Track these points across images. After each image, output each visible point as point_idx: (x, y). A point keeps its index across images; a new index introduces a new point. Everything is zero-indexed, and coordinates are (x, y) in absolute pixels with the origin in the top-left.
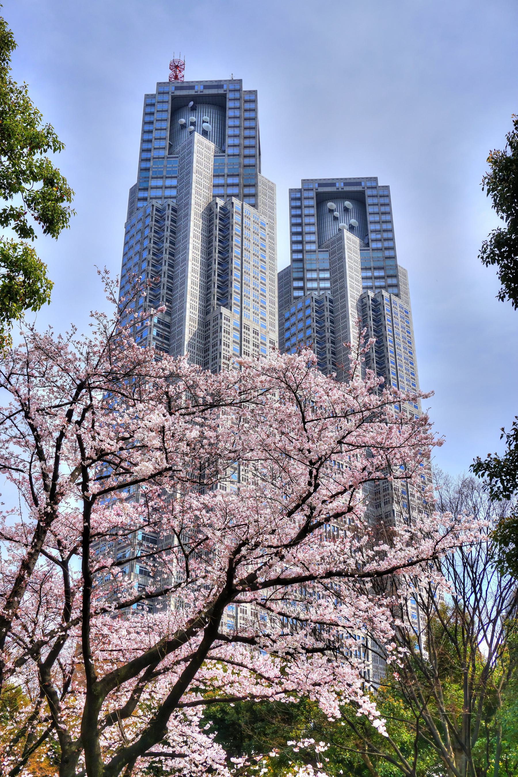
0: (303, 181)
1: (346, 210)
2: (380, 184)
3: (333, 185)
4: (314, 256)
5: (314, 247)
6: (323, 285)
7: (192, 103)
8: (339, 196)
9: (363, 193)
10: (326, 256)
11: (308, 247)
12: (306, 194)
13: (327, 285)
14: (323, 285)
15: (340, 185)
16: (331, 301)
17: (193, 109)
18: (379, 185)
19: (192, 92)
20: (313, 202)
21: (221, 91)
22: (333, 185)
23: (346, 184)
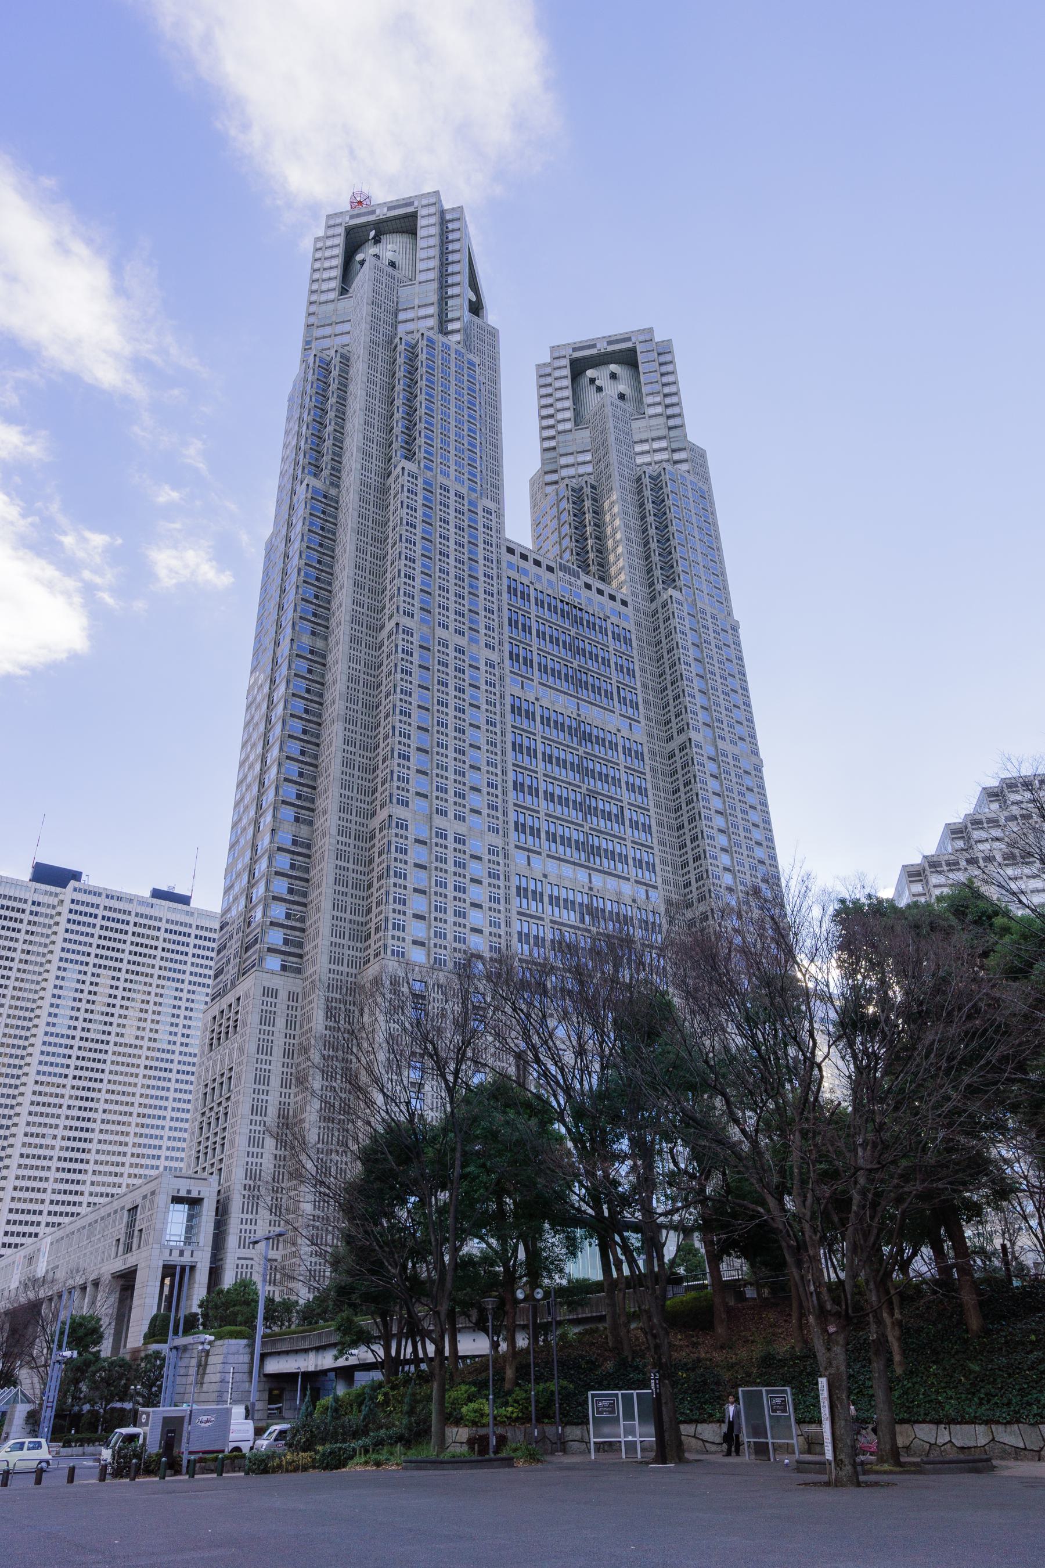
0: (553, 349)
1: (614, 376)
2: (658, 338)
3: (594, 346)
4: (569, 437)
5: (568, 426)
6: (582, 470)
7: (372, 234)
8: (600, 360)
9: (633, 351)
10: (586, 433)
11: (561, 427)
12: (557, 363)
13: (589, 469)
14: (582, 470)
15: (602, 347)
16: (593, 487)
17: (377, 240)
18: (657, 339)
19: (373, 218)
20: (567, 372)
21: (411, 209)
22: (594, 346)
23: (609, 343)
